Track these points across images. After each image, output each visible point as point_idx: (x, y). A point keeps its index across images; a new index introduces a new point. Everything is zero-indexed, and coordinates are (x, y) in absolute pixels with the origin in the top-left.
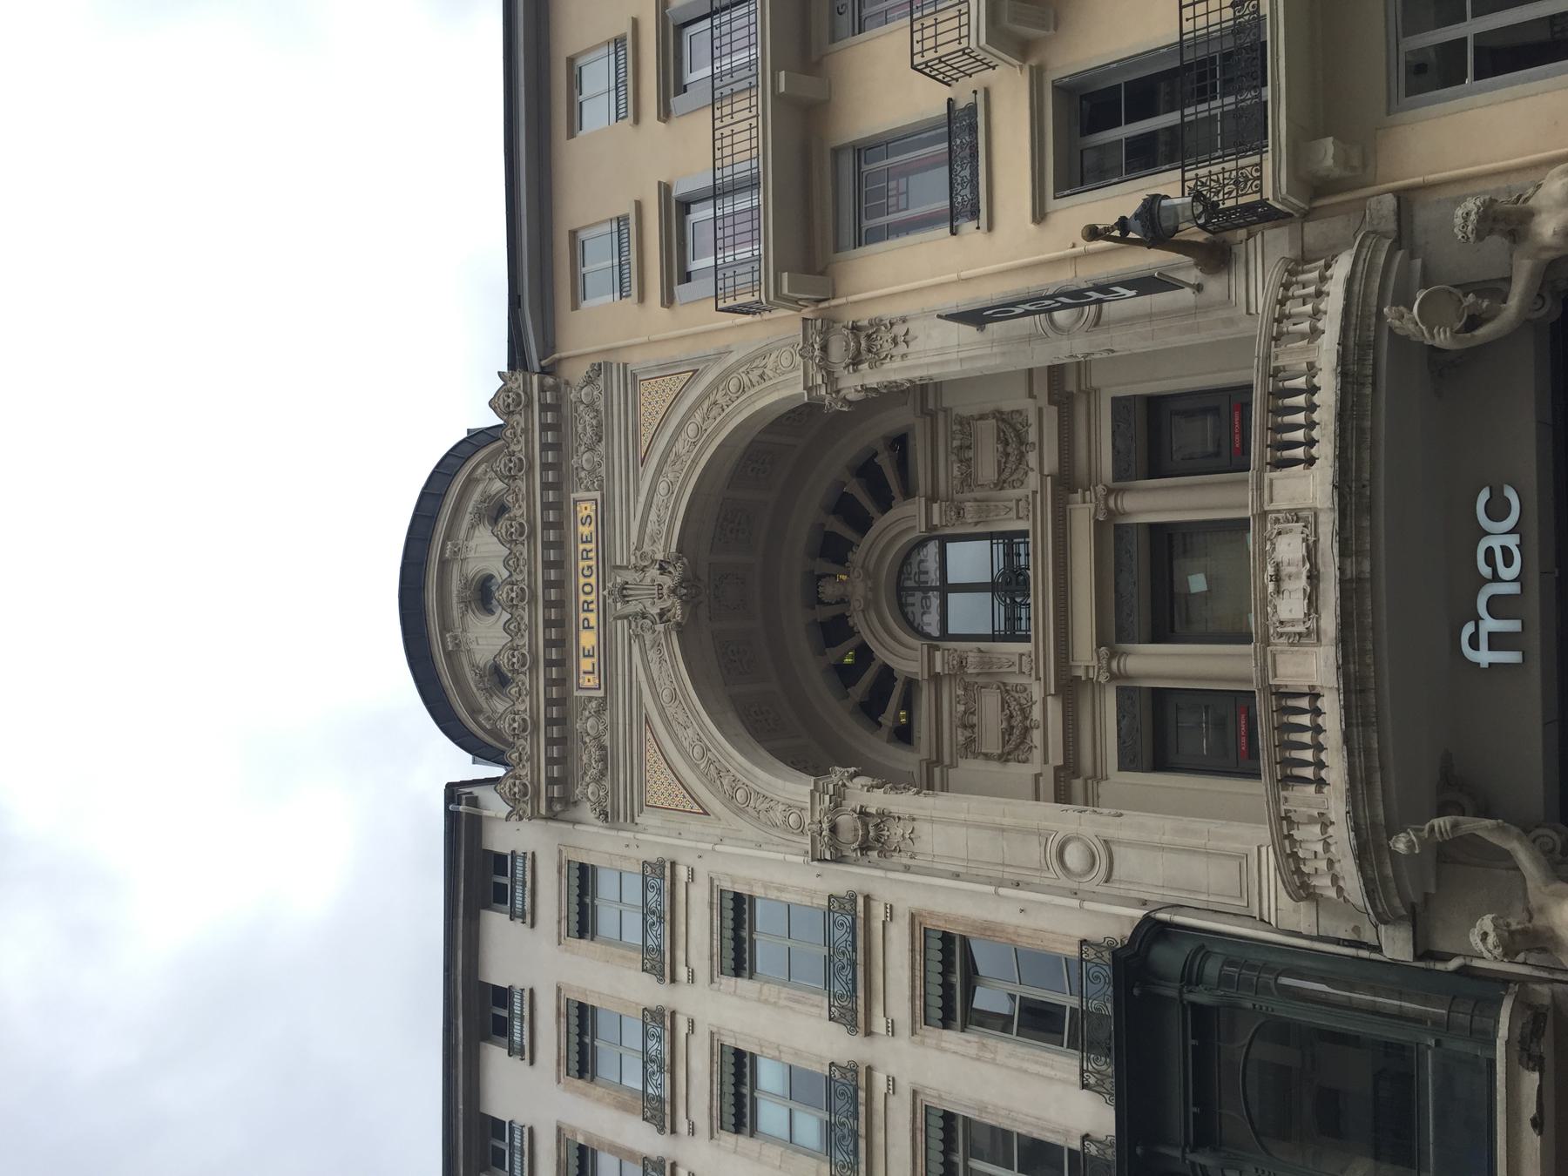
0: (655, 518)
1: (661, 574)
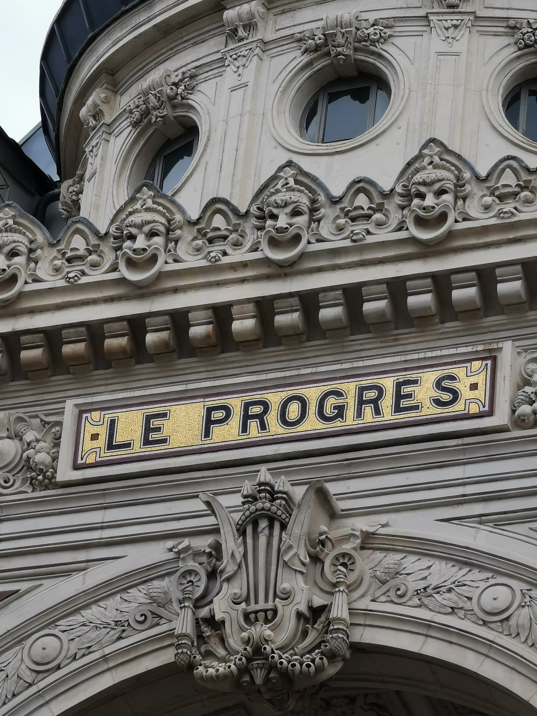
0: (434, 581)
1: (299, 615)
